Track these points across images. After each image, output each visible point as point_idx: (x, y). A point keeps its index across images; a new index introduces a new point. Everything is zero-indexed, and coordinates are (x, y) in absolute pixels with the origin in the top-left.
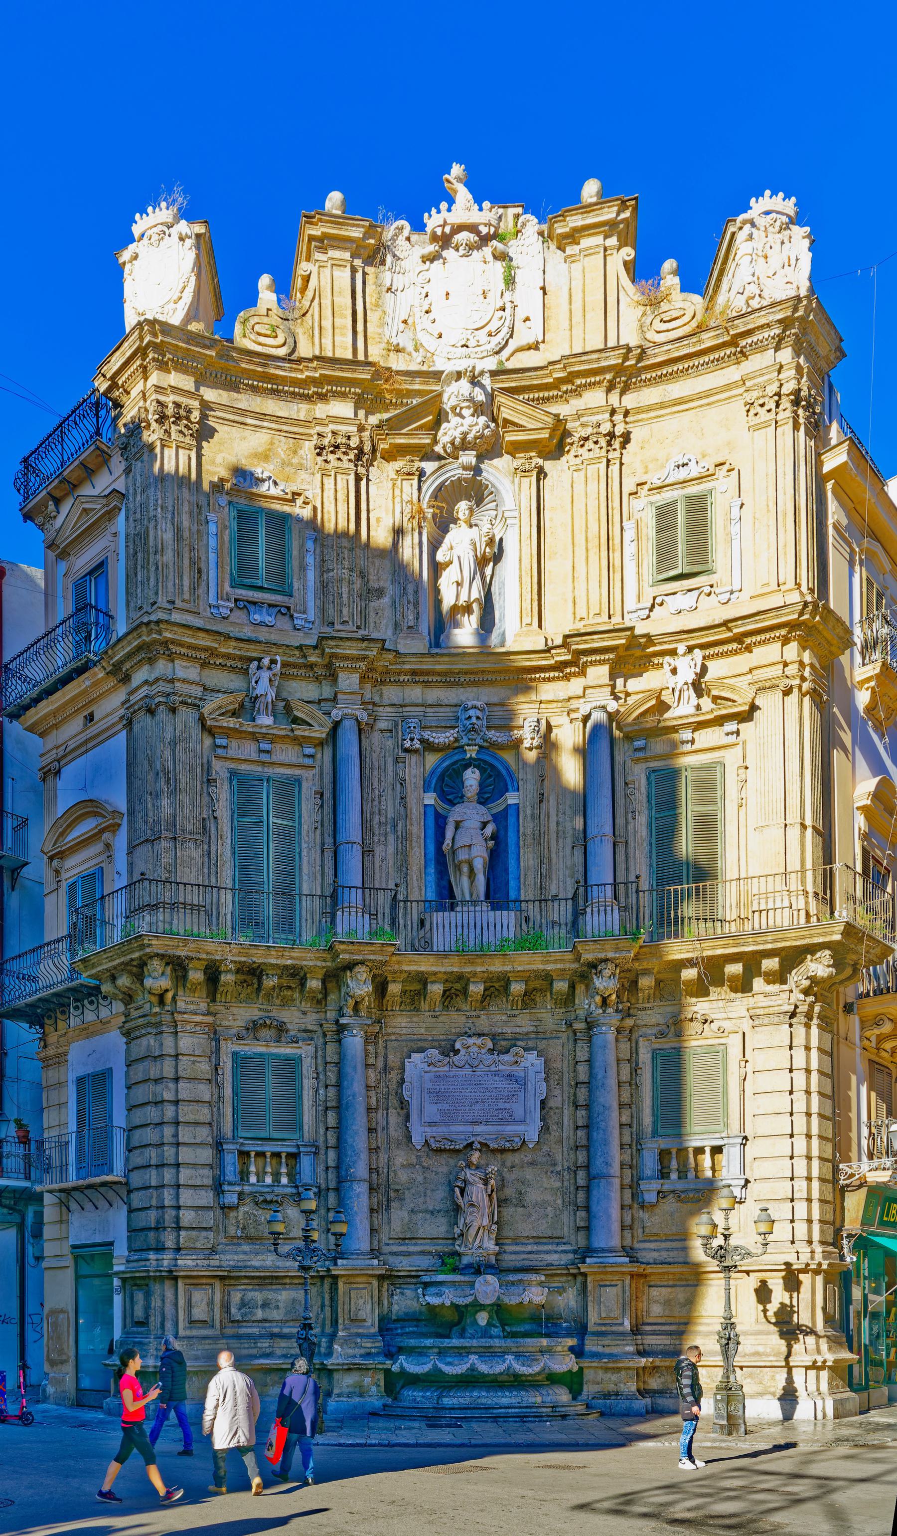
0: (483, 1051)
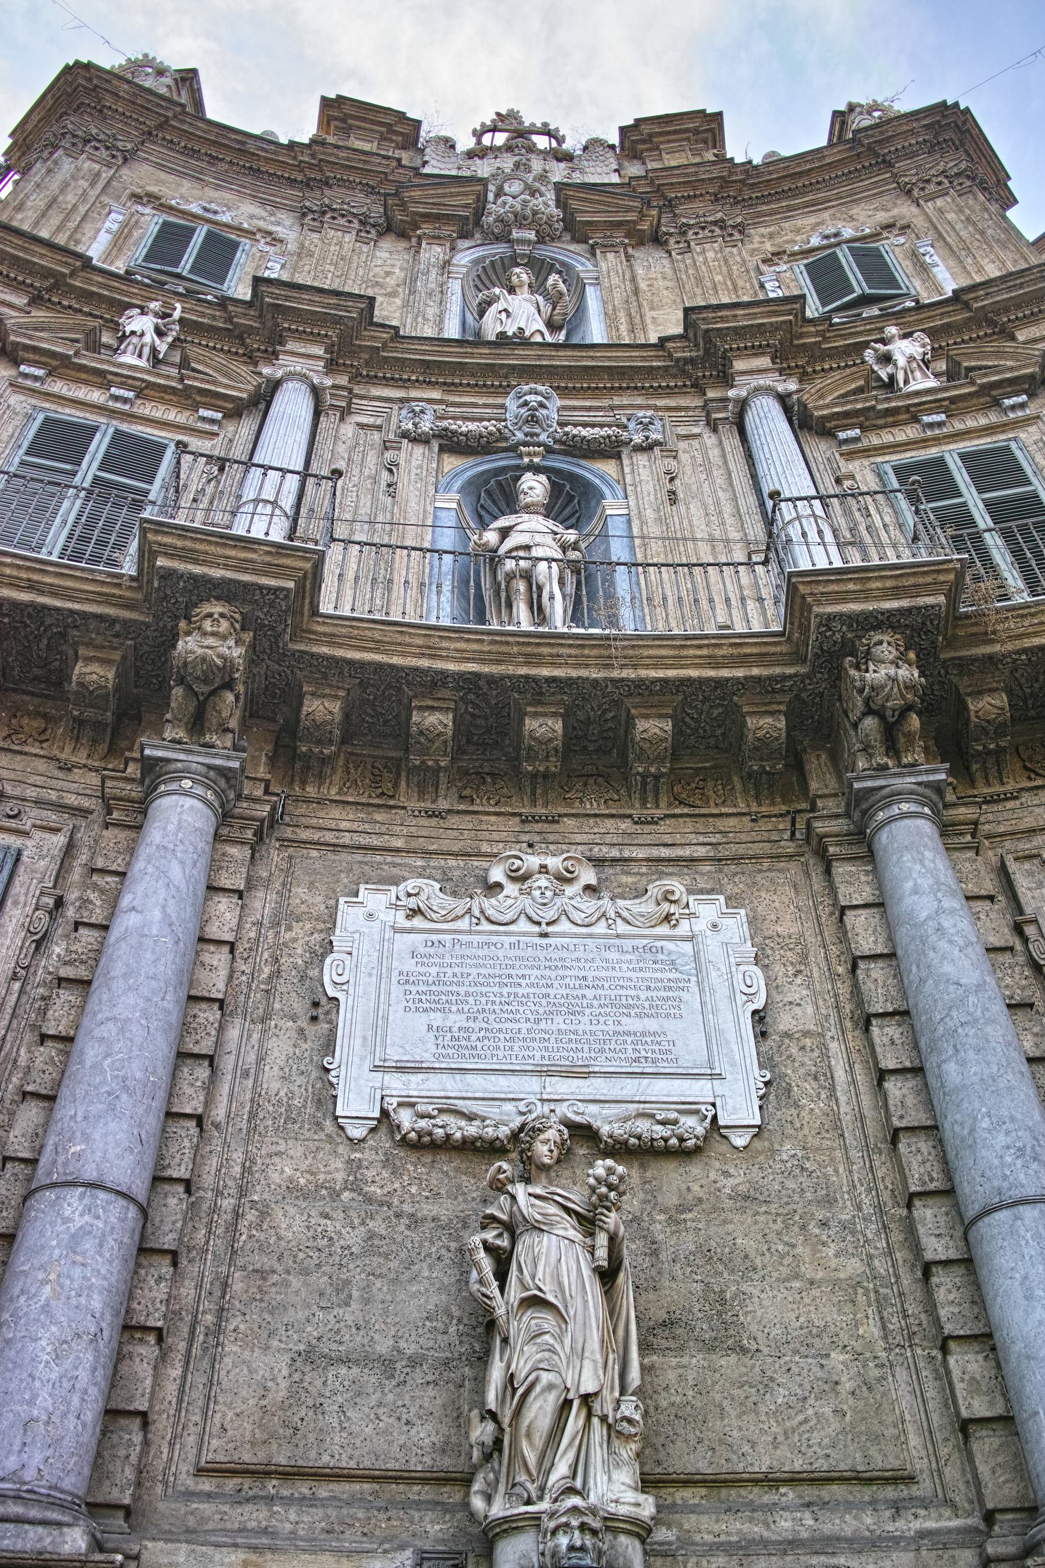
0: (570, 890)
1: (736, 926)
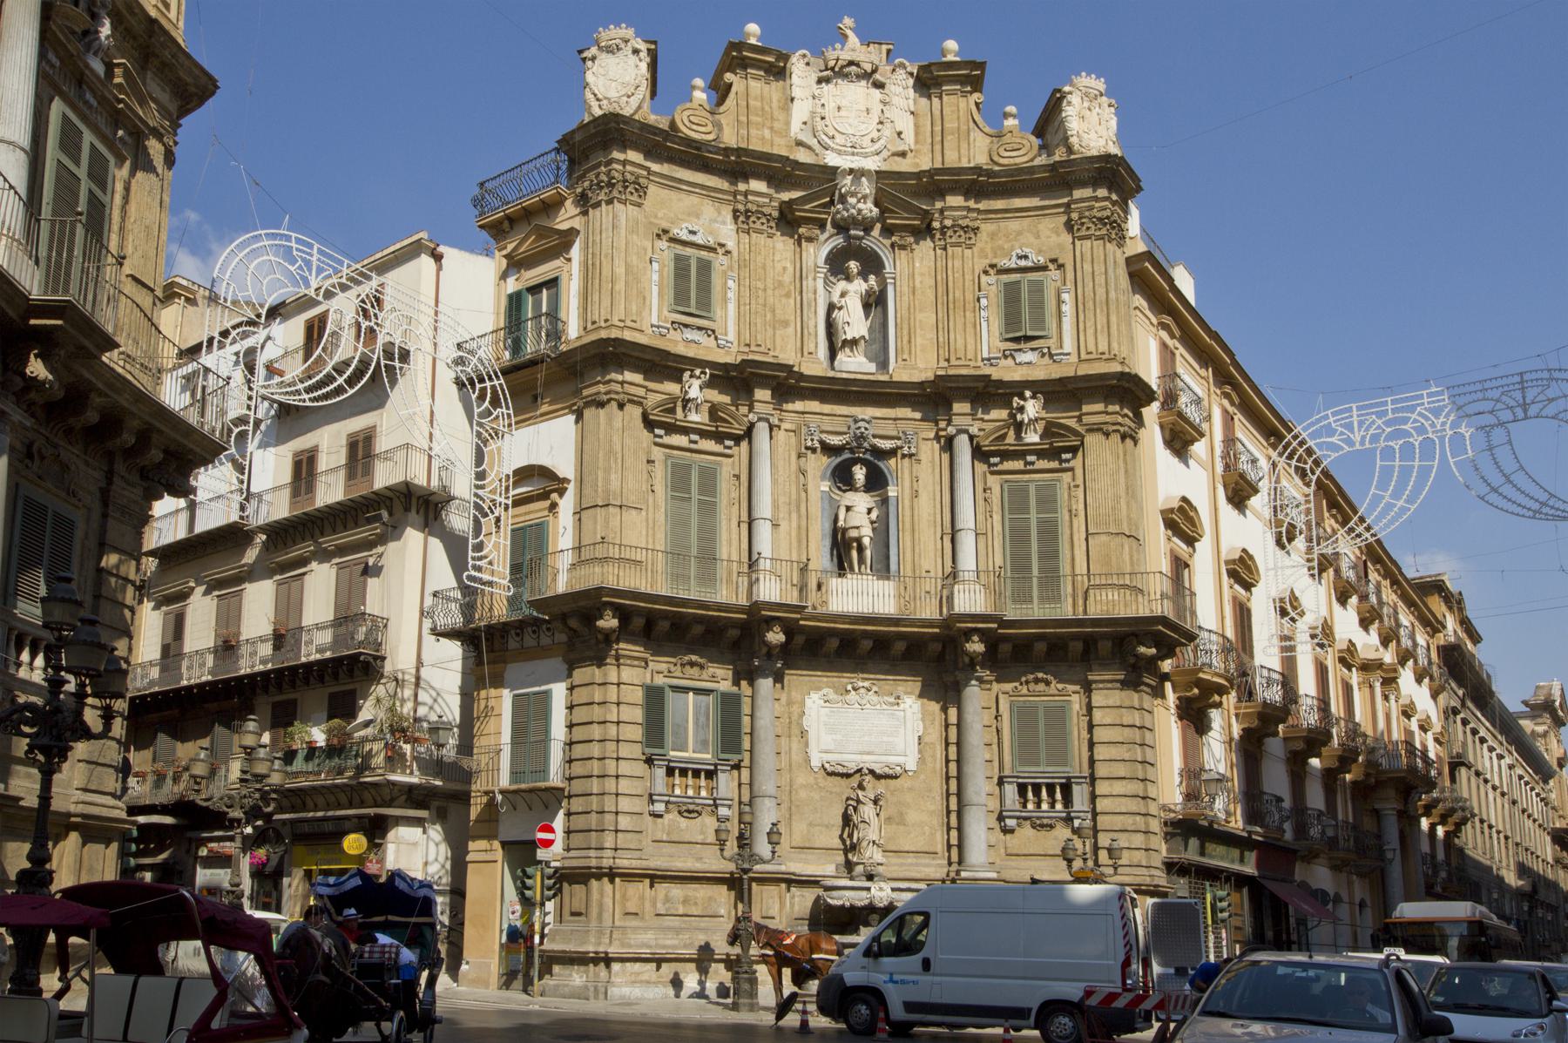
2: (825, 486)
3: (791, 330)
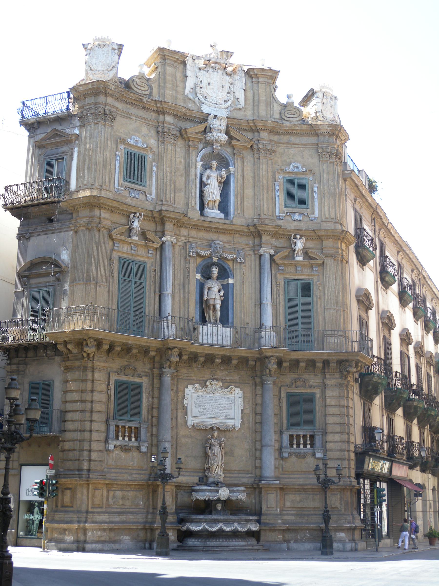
1: (241, 393)
2: (198, 276)
3: (182, 194)
